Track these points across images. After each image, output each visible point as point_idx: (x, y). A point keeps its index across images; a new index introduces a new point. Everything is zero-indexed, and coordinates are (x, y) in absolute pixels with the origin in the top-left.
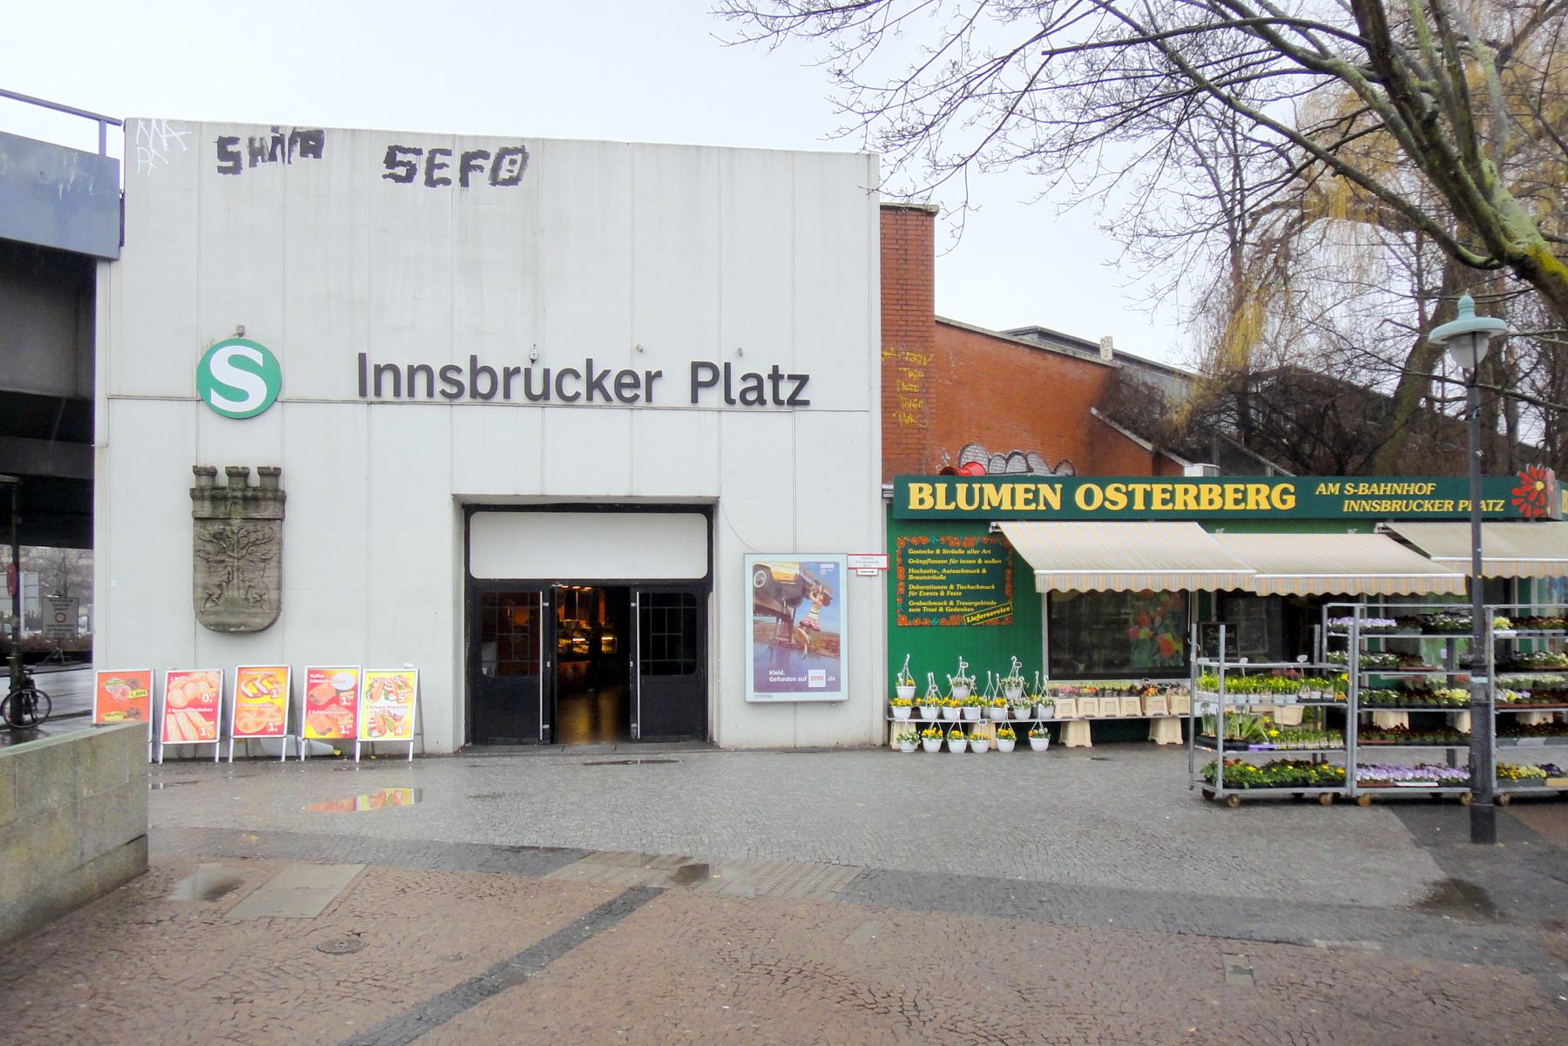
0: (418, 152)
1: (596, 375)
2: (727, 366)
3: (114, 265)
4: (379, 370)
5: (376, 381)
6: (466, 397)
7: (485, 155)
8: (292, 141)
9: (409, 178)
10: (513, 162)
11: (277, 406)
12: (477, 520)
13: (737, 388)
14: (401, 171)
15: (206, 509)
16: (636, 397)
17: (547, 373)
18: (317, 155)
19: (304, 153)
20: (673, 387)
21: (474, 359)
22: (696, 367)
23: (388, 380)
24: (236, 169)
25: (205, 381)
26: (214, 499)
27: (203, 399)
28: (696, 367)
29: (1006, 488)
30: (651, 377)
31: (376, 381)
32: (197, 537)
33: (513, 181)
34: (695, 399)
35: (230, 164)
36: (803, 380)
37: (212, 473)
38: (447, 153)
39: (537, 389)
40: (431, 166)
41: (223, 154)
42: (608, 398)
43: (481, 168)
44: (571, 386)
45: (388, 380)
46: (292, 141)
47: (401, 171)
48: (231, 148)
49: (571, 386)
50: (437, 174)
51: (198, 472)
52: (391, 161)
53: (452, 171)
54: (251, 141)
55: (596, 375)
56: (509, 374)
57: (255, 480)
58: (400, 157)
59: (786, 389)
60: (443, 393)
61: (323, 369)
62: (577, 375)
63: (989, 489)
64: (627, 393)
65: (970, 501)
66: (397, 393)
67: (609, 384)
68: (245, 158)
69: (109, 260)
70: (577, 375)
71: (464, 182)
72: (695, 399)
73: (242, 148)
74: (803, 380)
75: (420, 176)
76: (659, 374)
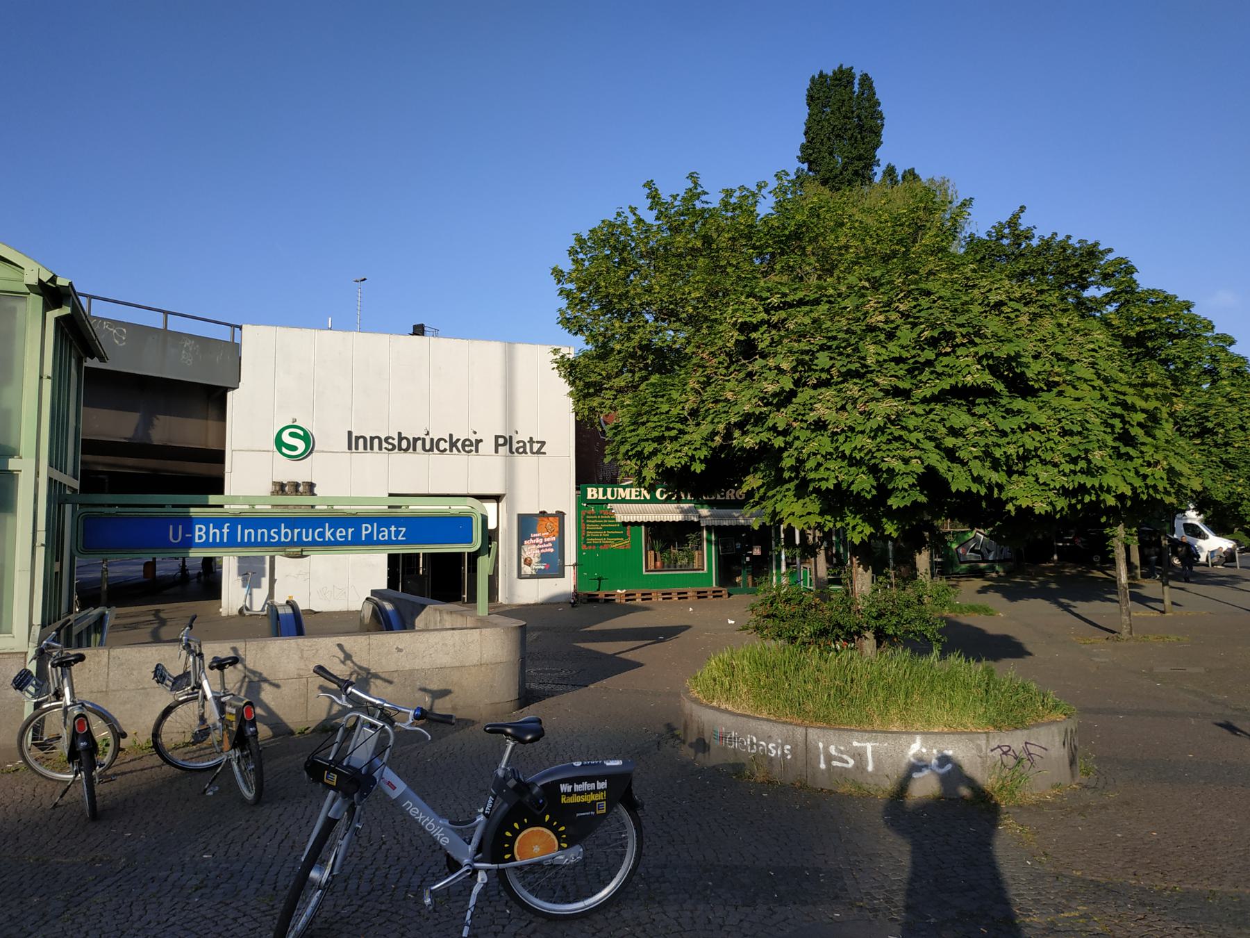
2: (511, 437)
4: (357, 438)
5: (353, 442)
13: (515, 446)
17: (432, 440)
20: (487, 446)
21: (400, 434)
22: (497, 437)
23: (361, 441)
25: (279, 443)
28: (497, 437)
29: (628, 490)
30: (478, 441)
31: (353, 442)
34: (497, 451)
36: (543, 443)
39: (428, 447)
44: (443, 445)
45: (361, 441)
49: (443, 445)
56: (416, 440)
59: (536, 447)
63: (621, 490)
66: (365, 448)
67: (459, 445)
72: (497, 451)
74: (543, 443)
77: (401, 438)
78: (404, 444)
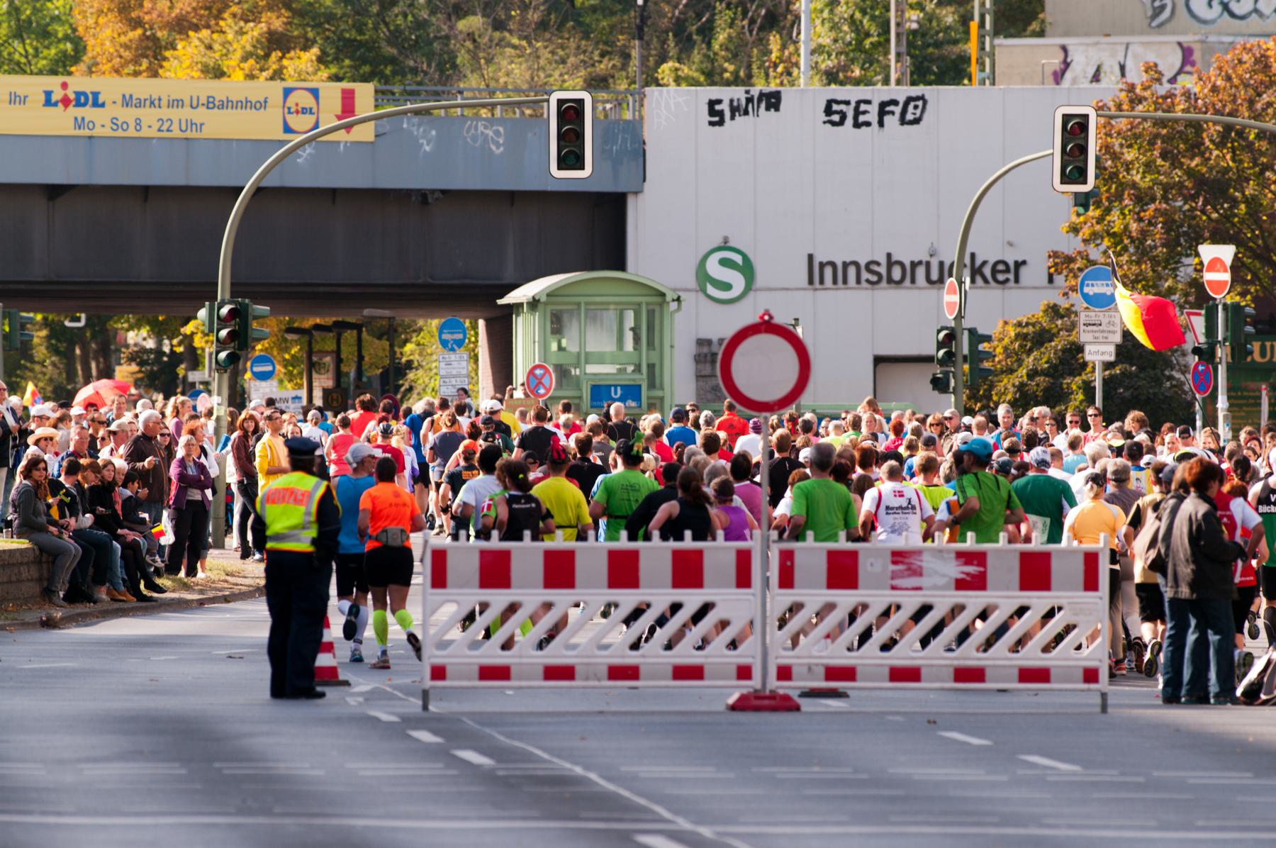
1: (978, 263)
3: (640, 196)
4: (822, 265)
6: (884, 284)
7: (895, 103)
8: (760, 100)
9: (841, 123)
10: (916, 107)
11: (752, 294)
12: (881, 366)
14: (836, 118)
16: (1007, 280)
17: (941, 264)
18: (777, 109)
19: (768, 109)
21: (889, 256)
23: (828, 272)
24: (721, 123)
25: (703, 278)
30: (1019, 265)
31: (819, 272)
32: (698, 389)
33: (917, 121)
34: (1051, 280)
35: (716, 119)
37: (709, 342)
38: (868, 102)
40: (857, 113)
41: (712, 112)
42: (986, 281)
43: (893, 113)
45: (828, 272)
46: (760, 100)
47: (836, 118)
48: (718, 107)
50: (862, 118)
51: (701, 342)
52: (828, 111)
53: (872, 116)
54: (732, 101)
55: (978, 263)
56: (914, 265)
60: (868, 281)
64: (1001, 277)
65: (1263, 354)
66: (835, 281)
67: (987, 271)
68: (727, 114)
69: (636, 193)
71: (881, 124)
73: (725, 107)
75: (849, 121)
76: (1024, 263)
77: (891, 263)
78: (897, 273)
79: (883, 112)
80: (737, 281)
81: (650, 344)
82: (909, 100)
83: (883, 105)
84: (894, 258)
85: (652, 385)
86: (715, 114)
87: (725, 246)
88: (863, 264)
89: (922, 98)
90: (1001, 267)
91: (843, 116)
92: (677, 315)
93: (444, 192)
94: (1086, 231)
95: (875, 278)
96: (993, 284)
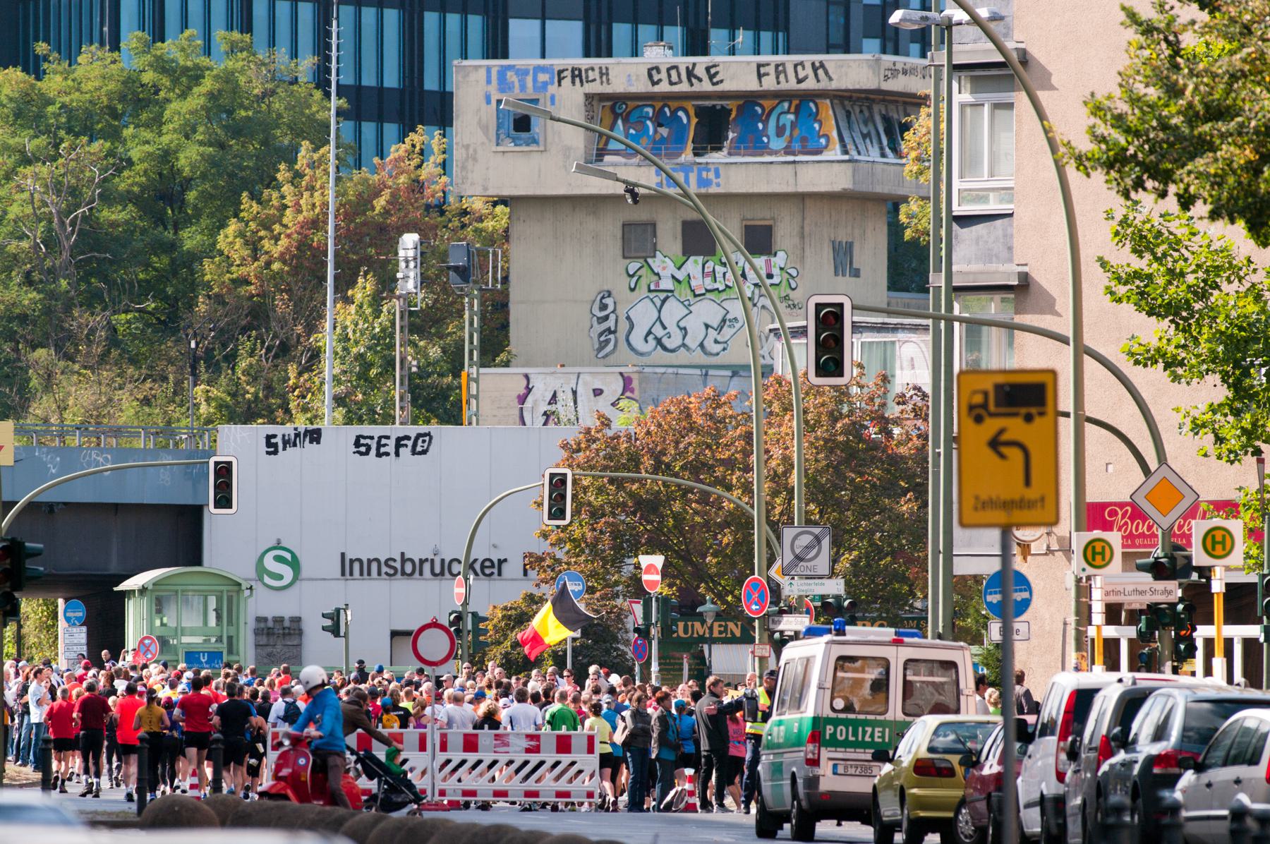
0: (372, 438)
4: (352, 561)
7: (408, 438)
8: (305, 436)
9: (367, 453)
10: (424, 441)
12: (396, 638)
14: (363, 449)
15: (264, 640)
16: (492, 573)
17: (443, 561)
18: (318, 443)
19: (311, 442)
21: (403, 554)
23: (356, 566)
24: (275, 453)
25: (261, 570)
26: (268, 634)
27: (261, 579)
31: (349, 567)
33: (424, 452)
34: (525, 573)
37: (265, 619)
38: (388, 437)
39: (437, 570)
40: (379, 445)
41: (269, 444)
42: (476, 574)
43: (406, 446)
44: (456, 568)
45: (356, 566)
46: (305, 436)
47: (363, 449)
48: (273, 441)
50: (383, 450)
52: (357, 444)
53: (391, 449)
56: (422, 562)
57: (287, 624)
58: (362, 441)
61: (320, 562)
62: (460, 562)
64: (488, 571)
65: (686, 632)
66: (361, 574)
67: (477, 566)
70: (460, 562)
71: (397, 454)
73: (279, 440)
75: (373, 452)
76: (505, 560)
77: (404, 560)
78: (409, 568)
79: (399, 444)
80: (288, 573)
81: (230, 622)
82: (419, 436)
83: (399, 440)
84: (407, 556)
85: (230, 652)
86: (271, 446)
87: (278, 546)
88: (383, 561)
89: (428, 434)
90: (487, 564)
91: (369, 448)
92: (249, 600)
93: (65, 504)
94: (553, 537)
95: (392, 572)
96: (481, 576)
